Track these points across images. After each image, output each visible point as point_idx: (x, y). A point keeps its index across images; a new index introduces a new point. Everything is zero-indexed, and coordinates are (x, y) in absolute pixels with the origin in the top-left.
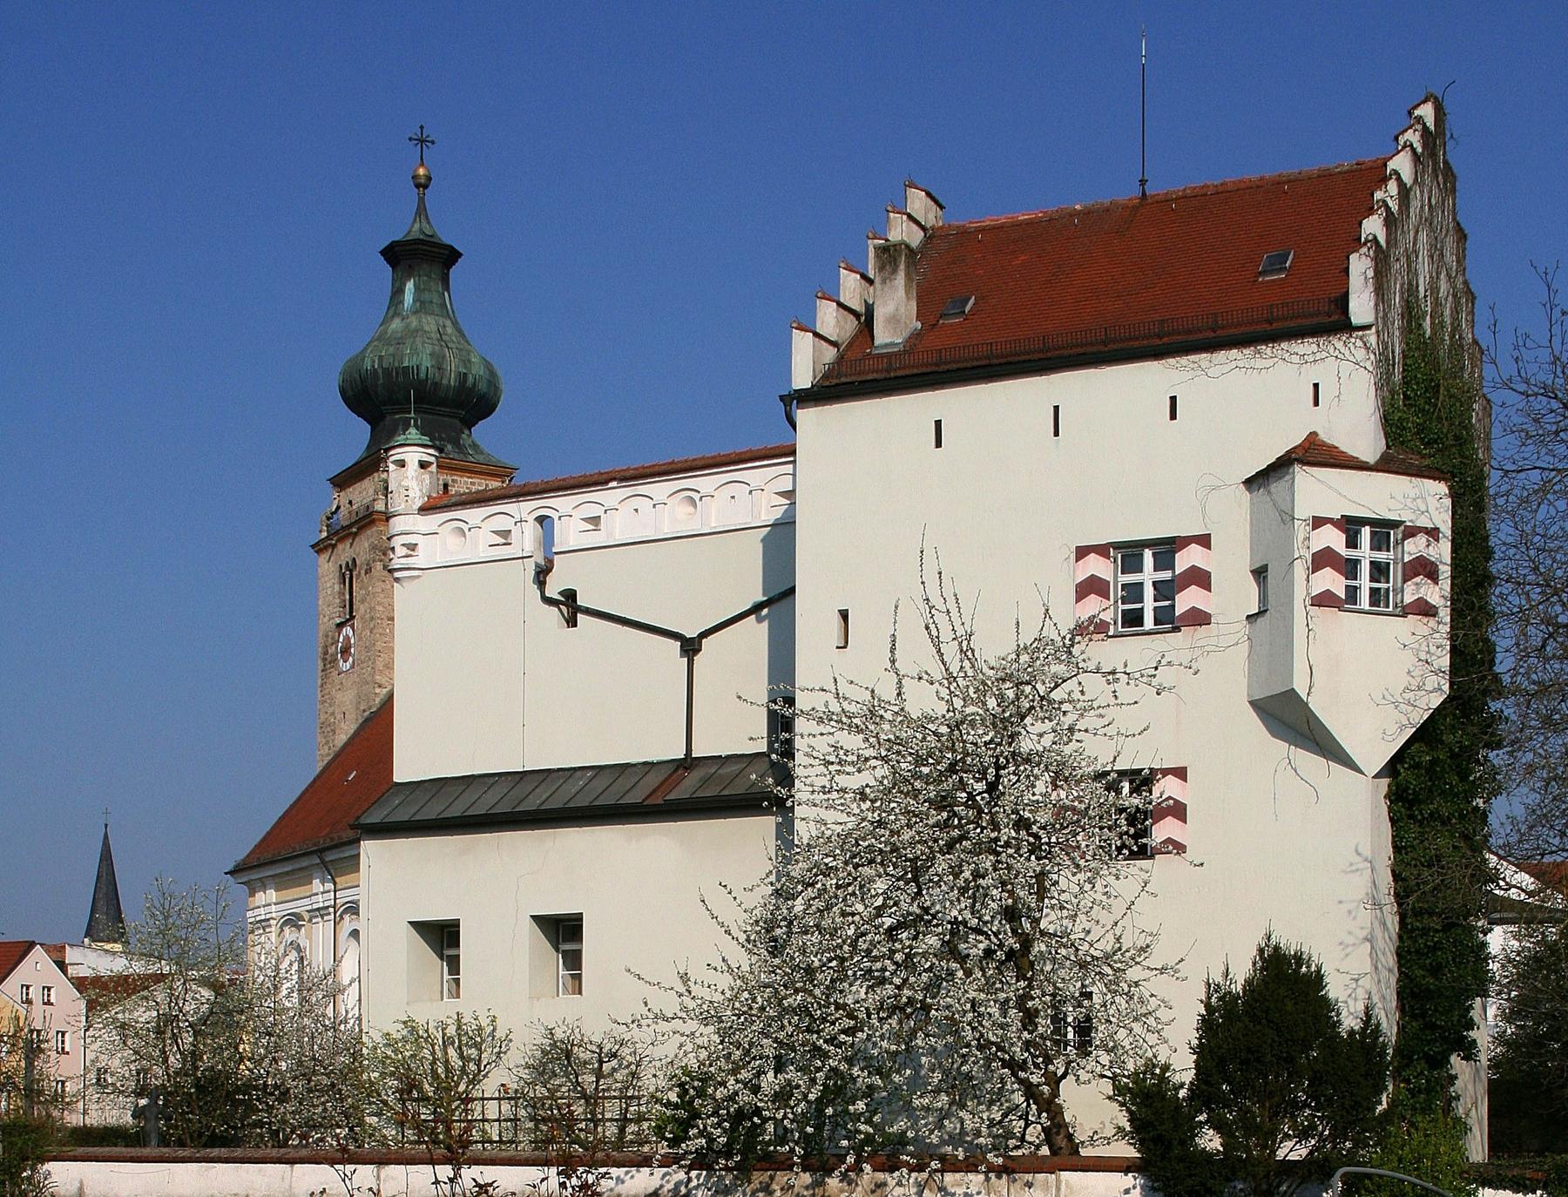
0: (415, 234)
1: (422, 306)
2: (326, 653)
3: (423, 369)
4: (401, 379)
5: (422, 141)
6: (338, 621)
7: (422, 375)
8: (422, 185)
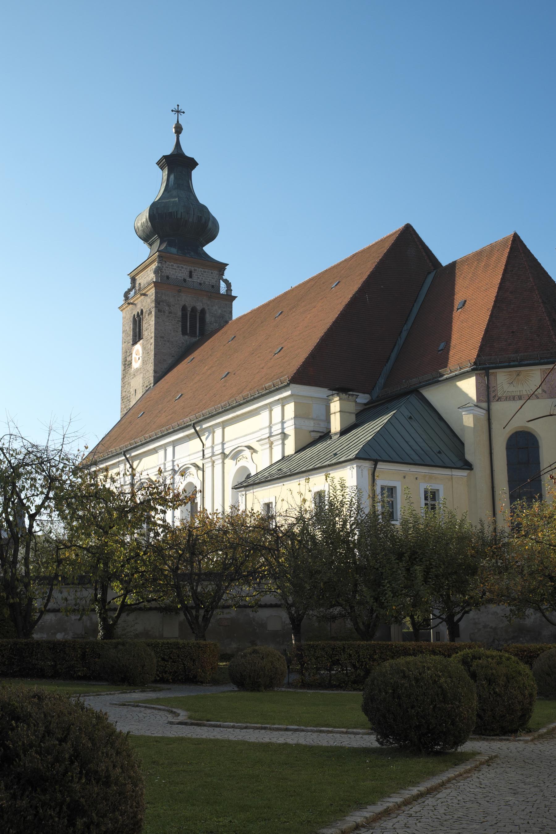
5: (178, 112)
7: (179, 216)
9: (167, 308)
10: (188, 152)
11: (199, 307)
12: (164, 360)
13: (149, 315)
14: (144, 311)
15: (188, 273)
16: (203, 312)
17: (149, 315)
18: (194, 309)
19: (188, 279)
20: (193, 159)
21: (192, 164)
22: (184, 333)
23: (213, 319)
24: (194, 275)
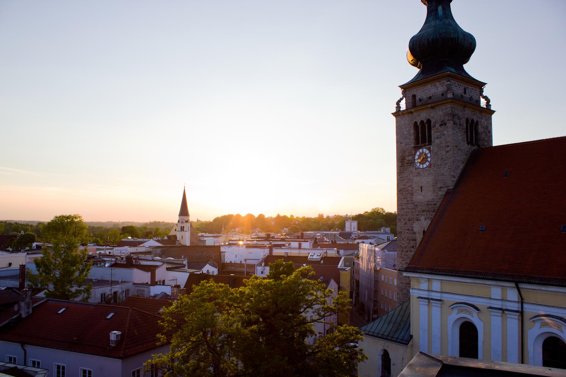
13: (441, 125)
14: (433, 121)
17: (441, 125)
22: (468, 143)
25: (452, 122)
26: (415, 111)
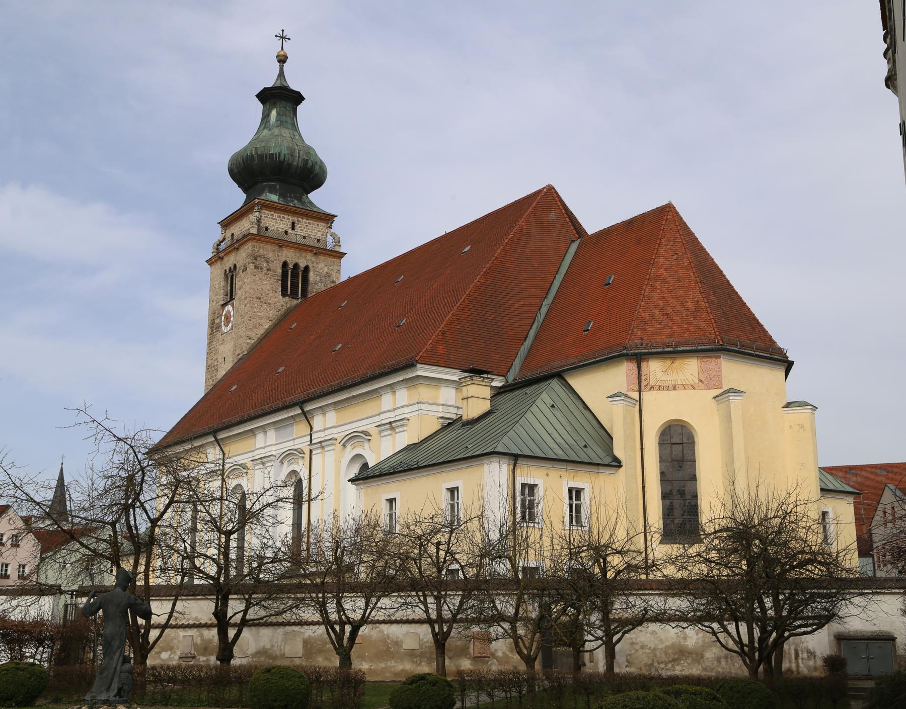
0: (278, 84)
1: (281, 123)
2: (213, 323)
3: (282, 155)
4: (268, 160)
5: (283, 38)
6: (222, 303)
7: (282, 159)
8: (282, 60)
9: (265, 264)
10: (294, 84)
11: (302, 265)
12: (260, 325)
14: (238, 266)
15: (290, 225)
16: (307, 269)
18: (296, 266)
19: (290, 231)
20: (299, 93)
21: (297, 98)
22: (284, 294)
23: (318, 279)
24: (297, 226)
25: (252, 266)
26: (225, 255)
